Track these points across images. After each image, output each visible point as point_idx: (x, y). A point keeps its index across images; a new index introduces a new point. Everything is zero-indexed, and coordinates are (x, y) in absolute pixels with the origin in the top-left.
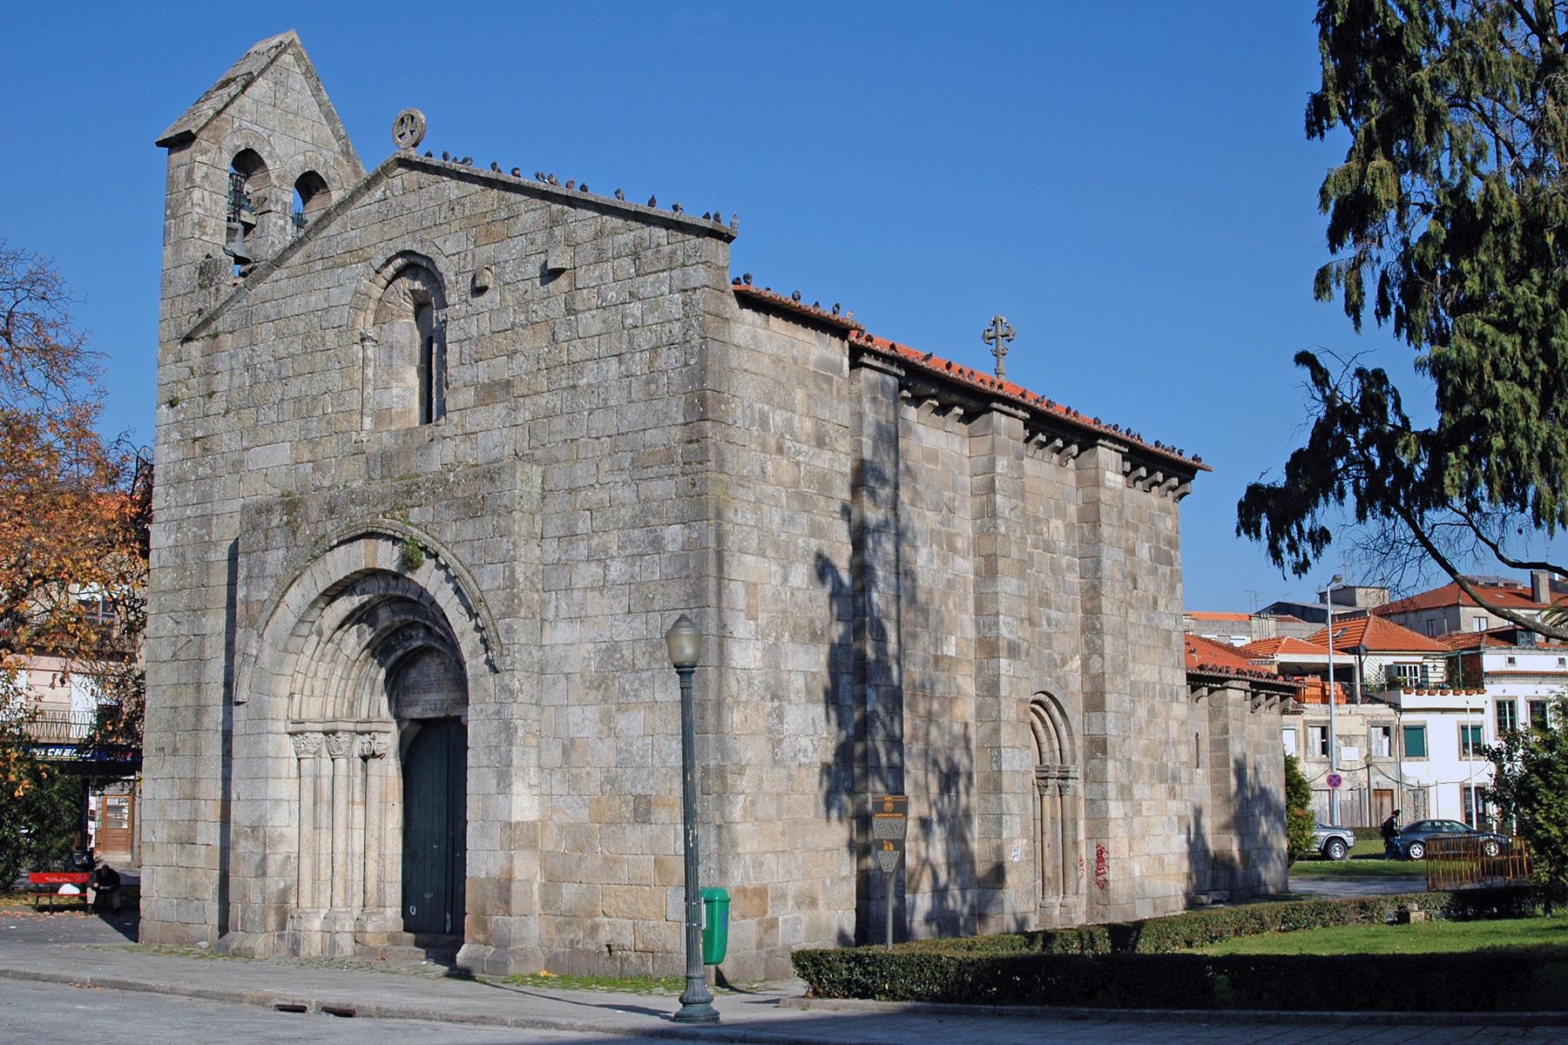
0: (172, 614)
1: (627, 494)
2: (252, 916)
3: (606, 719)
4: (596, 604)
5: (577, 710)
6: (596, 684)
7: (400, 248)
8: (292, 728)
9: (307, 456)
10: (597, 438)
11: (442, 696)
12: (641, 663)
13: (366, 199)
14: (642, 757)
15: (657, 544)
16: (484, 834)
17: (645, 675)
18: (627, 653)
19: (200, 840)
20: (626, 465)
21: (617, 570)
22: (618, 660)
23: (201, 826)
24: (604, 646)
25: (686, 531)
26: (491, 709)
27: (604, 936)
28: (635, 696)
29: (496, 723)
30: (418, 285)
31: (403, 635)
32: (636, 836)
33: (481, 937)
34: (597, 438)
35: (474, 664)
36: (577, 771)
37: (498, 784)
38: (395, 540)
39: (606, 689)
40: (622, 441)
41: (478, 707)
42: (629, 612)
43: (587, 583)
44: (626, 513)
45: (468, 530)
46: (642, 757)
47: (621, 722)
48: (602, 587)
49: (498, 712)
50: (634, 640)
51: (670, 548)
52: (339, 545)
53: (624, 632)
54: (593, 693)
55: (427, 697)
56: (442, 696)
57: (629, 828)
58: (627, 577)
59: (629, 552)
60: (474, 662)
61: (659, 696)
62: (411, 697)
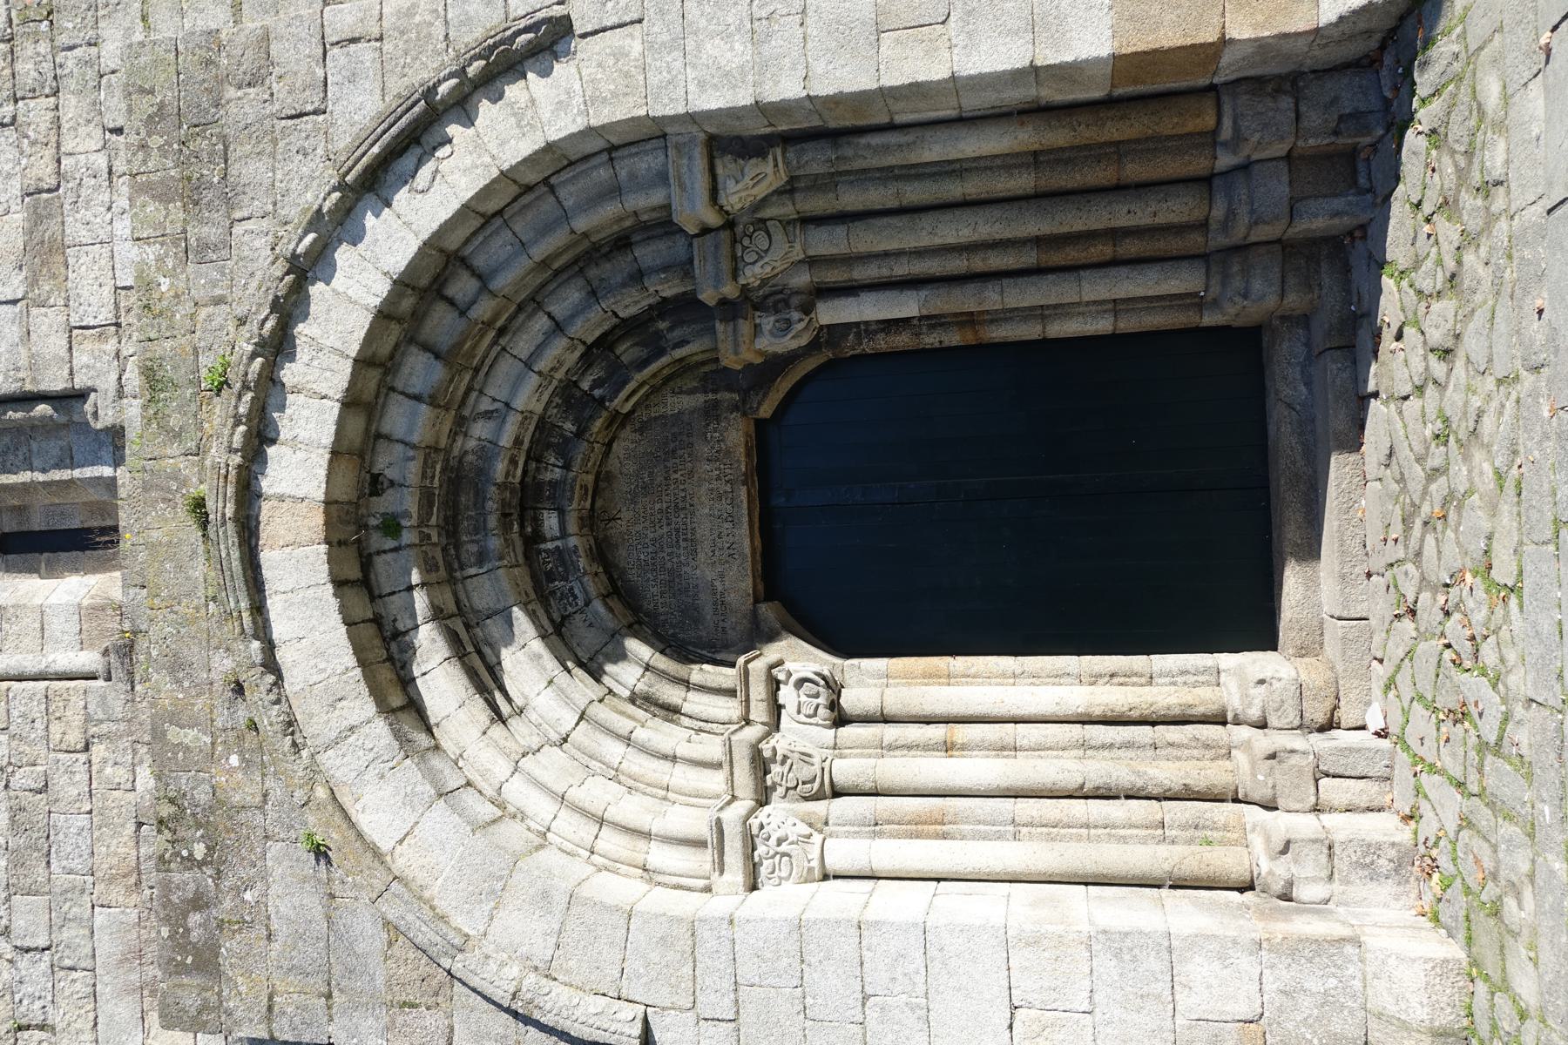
8: (735, 874)
31: (550, 577)
52: (262, 630)
60: (545, 112)
62: (705, 599)
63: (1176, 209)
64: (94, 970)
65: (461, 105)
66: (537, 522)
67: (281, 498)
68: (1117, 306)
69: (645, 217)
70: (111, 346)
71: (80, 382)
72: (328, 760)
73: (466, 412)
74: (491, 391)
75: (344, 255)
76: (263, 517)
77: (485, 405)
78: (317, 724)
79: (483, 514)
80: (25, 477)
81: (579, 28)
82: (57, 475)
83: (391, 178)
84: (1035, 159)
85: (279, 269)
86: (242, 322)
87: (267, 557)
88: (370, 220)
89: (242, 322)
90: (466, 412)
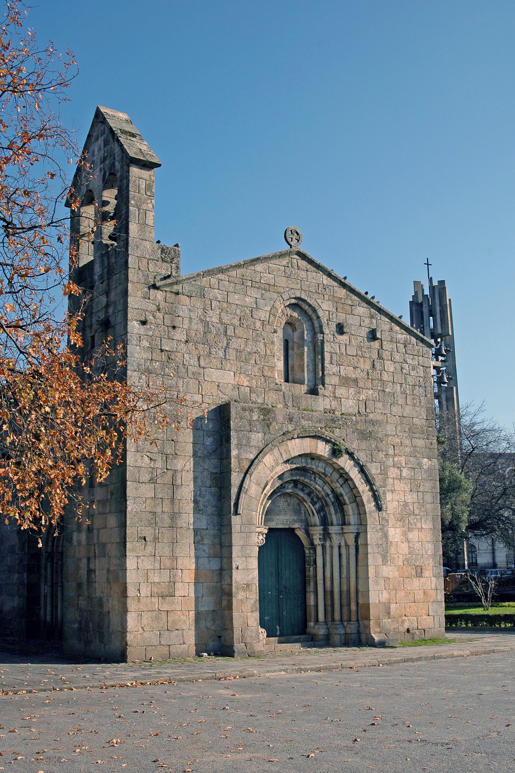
0: (148, 454)
1: (407, 442)
2: (250, 633)
3: (404, 534)
4: (399, 486)
5: (393, 529)
6: (399, 519)
7: (298, 295)
9: (246, 383)
10: (395, 416)
11: (287, 518)
12: (417, 512)
13: (277, 261)
14: (419, 550)
15: (420, 464)
16: (377, 583)
17: (418, 517)
18: (411, 507)
19: (177, 594)
20: (407, 430)
21: (405, 472)
22: (408, 510)
23: (178, 585)
24: (402, 503)
25: (430, 462)
26: (379, 527)
27: (406, 625)
28: (415, 525)
29: (380, 534)
30: (295, 315)
32: (416, 583)
33: (378, 630)
34: (395, 416)
35: (370, 506)
36: (394, 555)
37: (383, 561)
38: (327, 441)
39: (404, 522)
40: (404, 420)
41: (372, 526)
42: (411, 491)
43: (394, 476)
44: (408, 450)
45: (364, 445)
46: (419, 550)
47: (410, 536)
48: (401, 478)
49: (381, 529)
50: (413, 503)
51: (424, 467)
53: (410, 498)
54: (399, 523)
55: (278, 517)
56: (287, 518)
57: (415, 579)
58: (409, 476)
59: (410, 466)
60: (369, 505)
61: (423, 526)
63: (337, 616)
64: (222, 369)
65: (372, 489)
66: (290, 483)
67: (317, 444)
68: (316, 606)
69: (346, 517)
70: (332, 395)
71: (326, 385)
72: (276, 449)
73: (316, 475)
74: (319, 480)
75: (352, 462)
76: (314, 440)
77: (317, 479)
78: (283, 449)
79: (296, 475)
80: (306, 360)
81: (380, 512)
82: (306, 369)
83: (362, 474)
84: (349, 591)
85: (352, 451)
86: (344, 440)
87: (308, 439)
88: (357, 469)
89: (344, 440)
90: (316, 475)
